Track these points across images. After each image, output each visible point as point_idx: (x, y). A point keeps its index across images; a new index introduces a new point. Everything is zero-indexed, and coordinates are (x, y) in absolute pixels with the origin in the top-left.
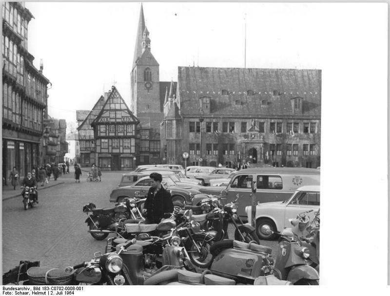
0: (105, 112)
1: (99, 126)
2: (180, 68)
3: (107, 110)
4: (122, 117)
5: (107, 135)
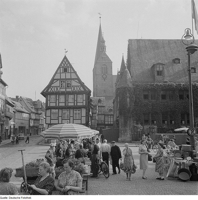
0: (55, 81)
1: (49, 96)
2: (130, 41)
3: (57, 80)
5: (57, 105)
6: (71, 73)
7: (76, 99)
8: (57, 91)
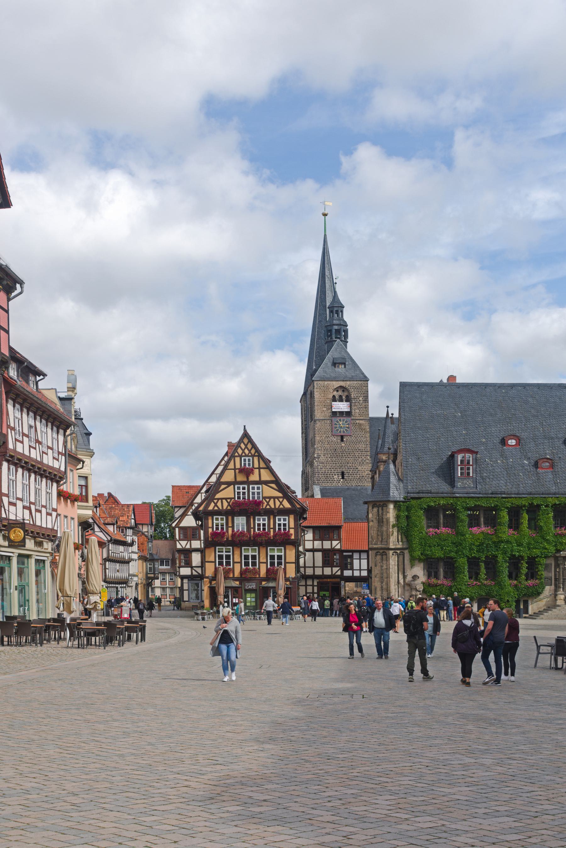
0: (223, 486)
1: (210, 518)
3: (229, 484)
4: (264, 498)
7: (272, 526)
8: (229, 508)
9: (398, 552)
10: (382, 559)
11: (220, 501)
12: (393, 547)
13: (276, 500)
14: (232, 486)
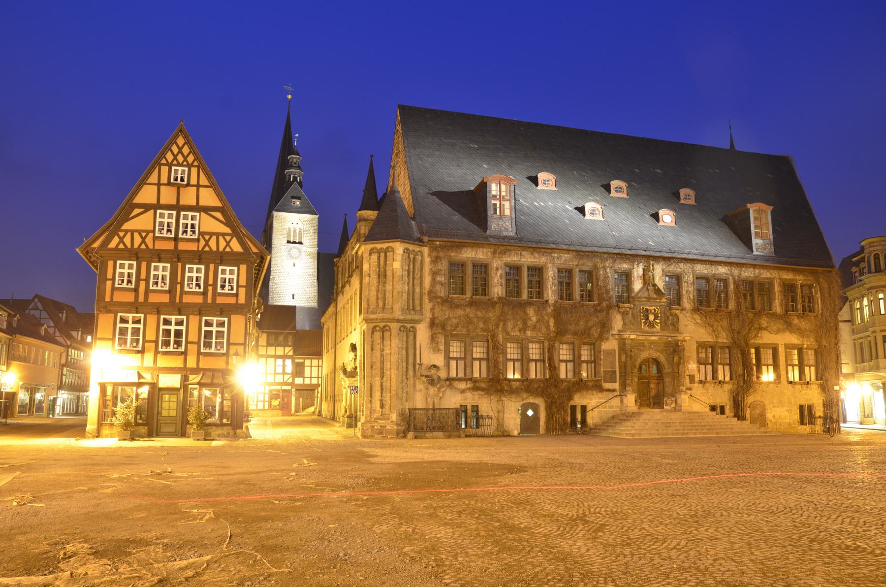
0: (137, 211)
1: (110, 264)
3: (146, 207)
6: (198, 186)
7: (211, 282)
8: (143, 246)
9: (409, 326)
10: (383, 338)
11: (129, 234)
12: (401, 318)
13: (221, 238)
14: (152, 211)
